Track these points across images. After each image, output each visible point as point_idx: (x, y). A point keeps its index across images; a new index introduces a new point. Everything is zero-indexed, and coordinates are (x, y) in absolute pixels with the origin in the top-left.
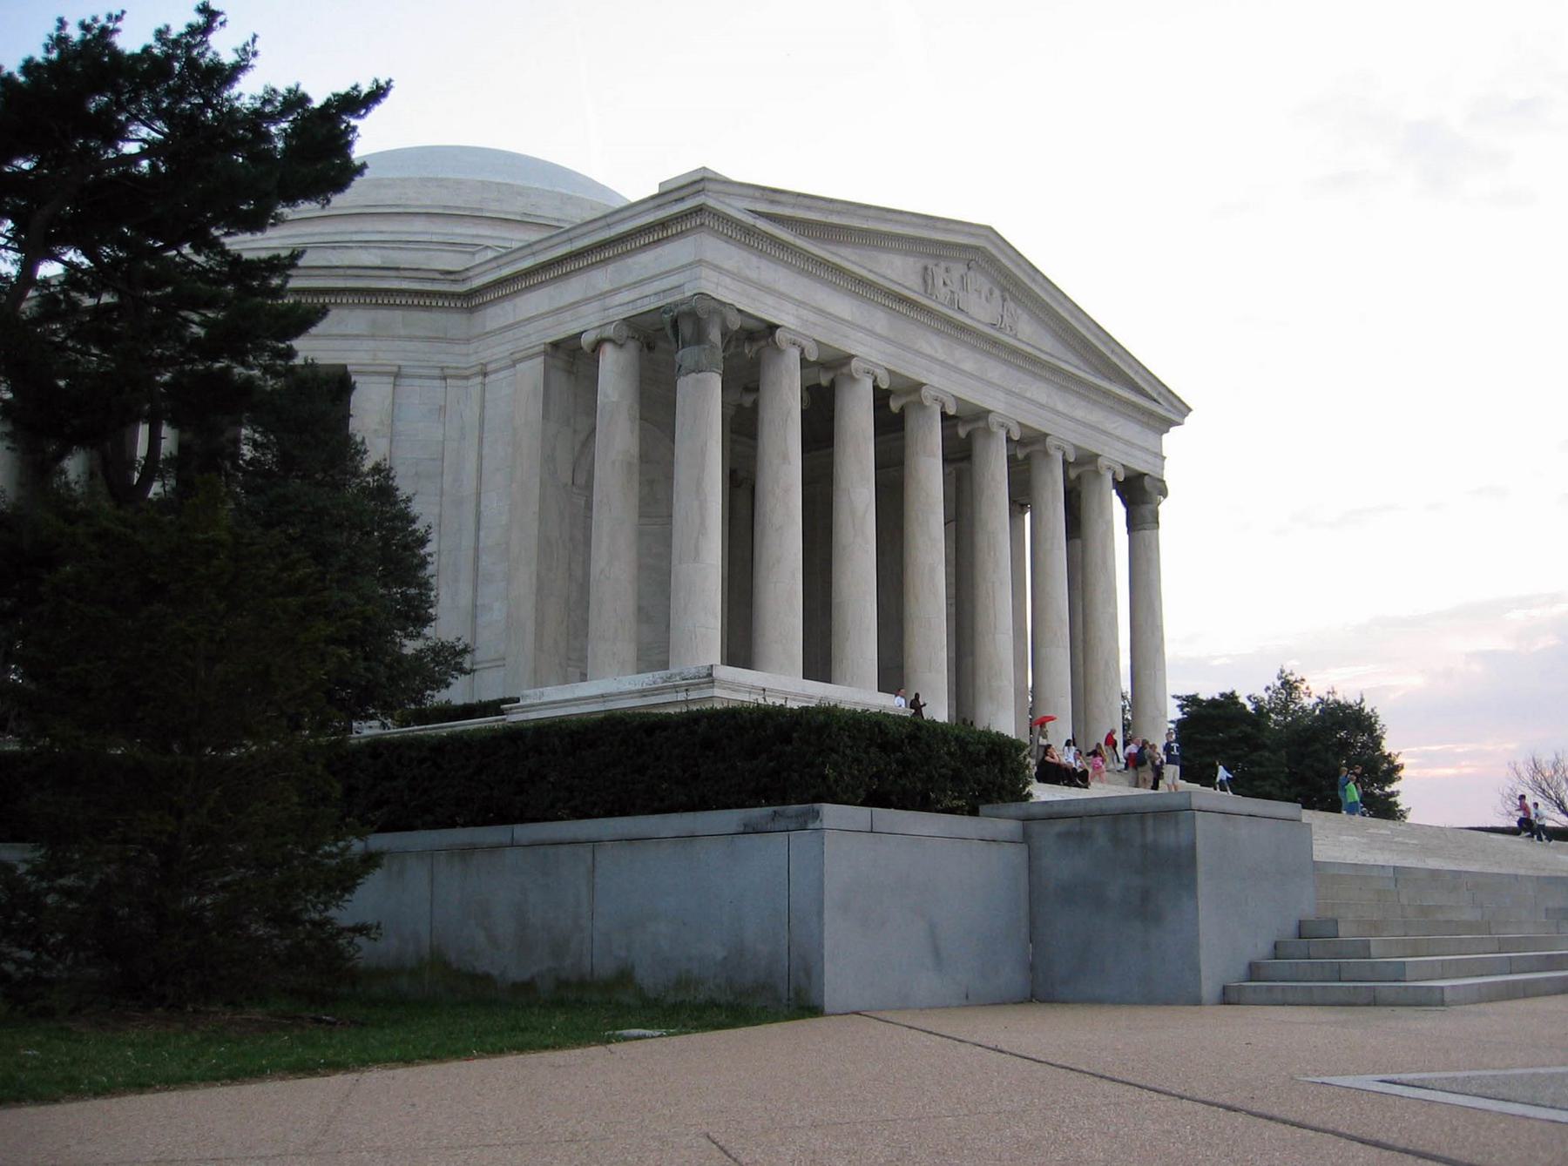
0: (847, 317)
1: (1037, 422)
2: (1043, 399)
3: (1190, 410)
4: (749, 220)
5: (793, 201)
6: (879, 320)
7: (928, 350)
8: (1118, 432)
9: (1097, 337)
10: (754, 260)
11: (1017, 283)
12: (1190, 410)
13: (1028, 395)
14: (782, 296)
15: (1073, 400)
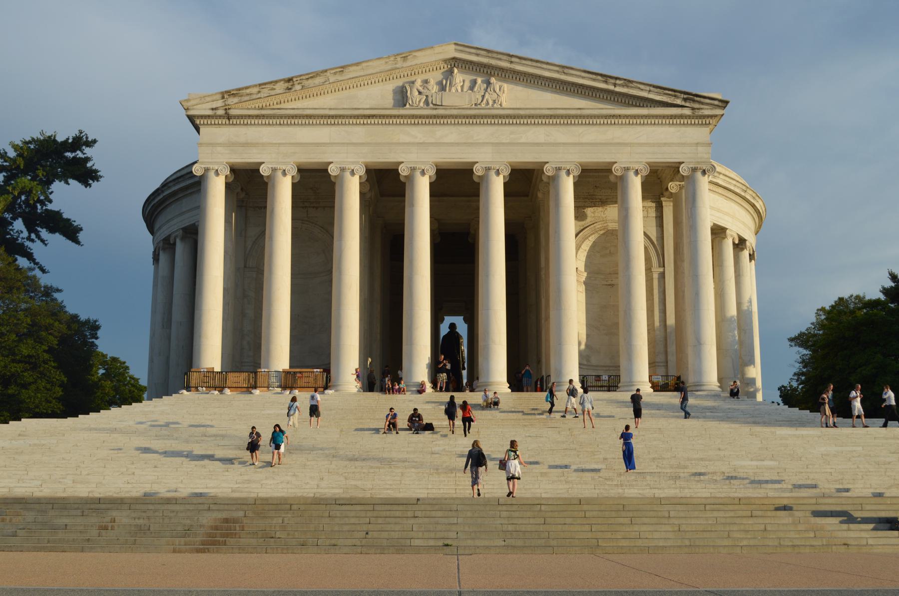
0: (326, 140)
1: (526, 157)
2: (542, 139)
3: (727, 102)
4: (221, 112)
5: (255, 90)
6: (358, 133)
7: (407, 139)
8: (643, 140)
9: (594, 80)
10: (242, 130)
11: (502, 69)
12: (727, 102)
13: (522, 140)
14: (263, 144)
15: (581, 129)
